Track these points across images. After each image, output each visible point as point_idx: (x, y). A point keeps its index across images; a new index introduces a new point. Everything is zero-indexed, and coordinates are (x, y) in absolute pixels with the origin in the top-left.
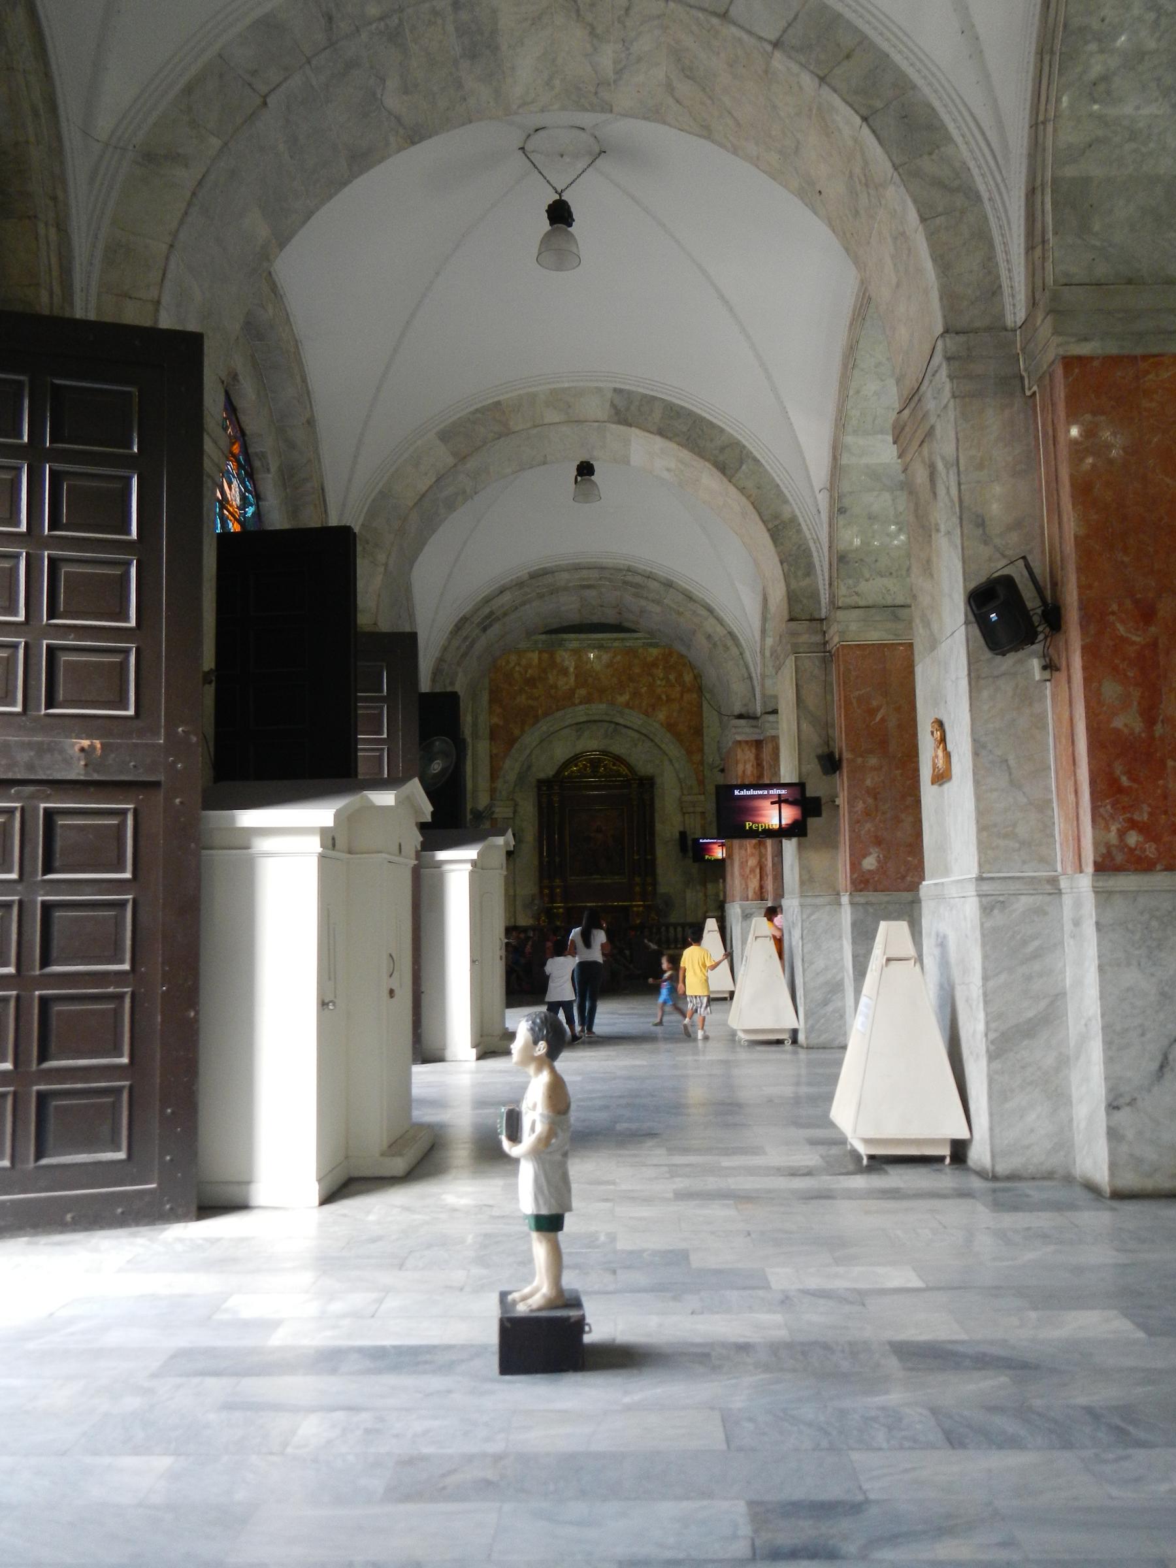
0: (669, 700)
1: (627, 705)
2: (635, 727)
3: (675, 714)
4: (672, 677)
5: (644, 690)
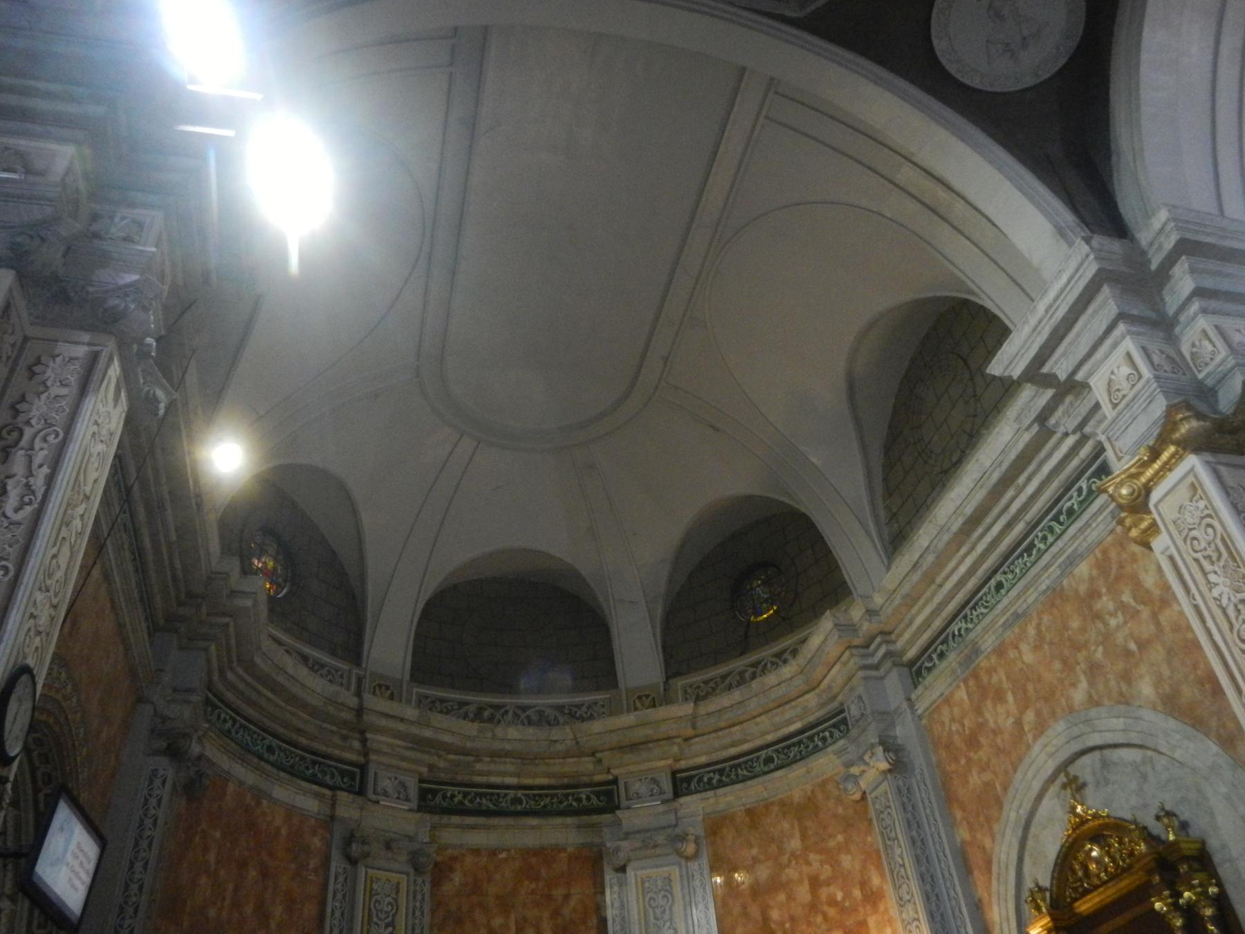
0: (1143, 645)
1: (1093, 702)
2: (1120, 739)
3: (1166, 672)
4: (1126, 598)
5: (1099, 654)
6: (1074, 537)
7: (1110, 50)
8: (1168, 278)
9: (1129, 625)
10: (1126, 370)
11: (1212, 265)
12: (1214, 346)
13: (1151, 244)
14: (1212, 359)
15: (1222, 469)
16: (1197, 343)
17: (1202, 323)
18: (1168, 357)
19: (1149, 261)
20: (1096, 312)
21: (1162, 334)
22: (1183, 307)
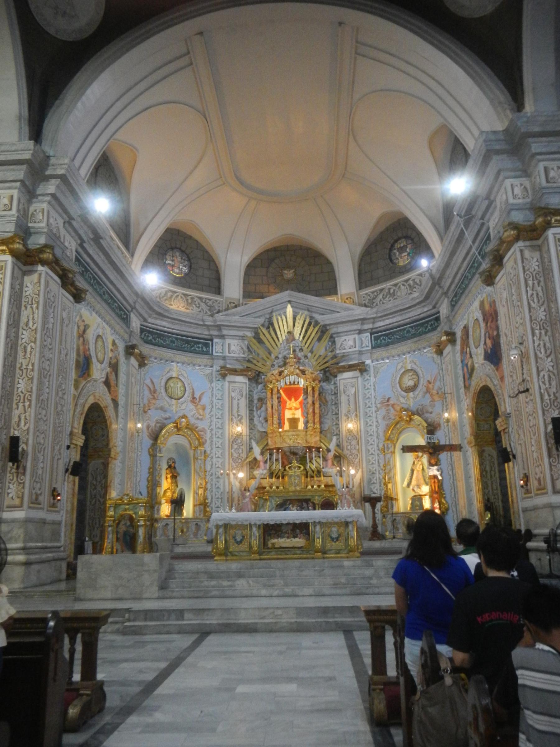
7: (89, 59)
8: (48, 181)
10: (6, 201)
11: (64, 188)
12: (43, 218)
13: (53, 165)
14: (38, 222)
15: (16, 267)
16: (38, 211)
17: (45, 205)
18: (24, 208)
19: (47, 169)
20: (14, 170)
21: (28, 197)
22: (43, 195)
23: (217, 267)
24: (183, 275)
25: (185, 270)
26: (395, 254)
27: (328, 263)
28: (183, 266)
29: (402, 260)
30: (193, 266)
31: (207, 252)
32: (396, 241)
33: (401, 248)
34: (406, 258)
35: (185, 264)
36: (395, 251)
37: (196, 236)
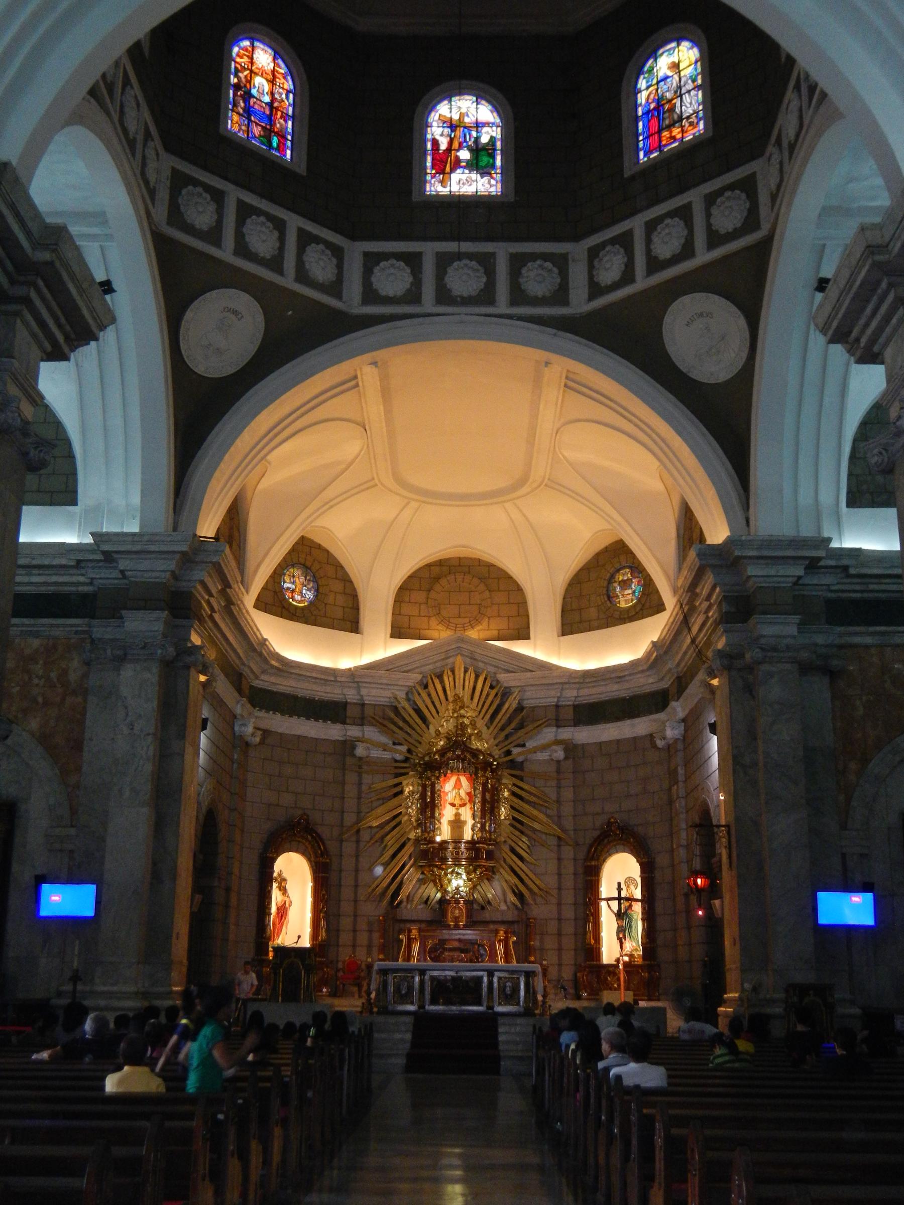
4: (53, 675)
6: (43, 625)
9: (46, 689)
23: (355, 590)
24: (306, 604)
25: (310, 595)
26: (615, 589)
27: (519, 589)
28: (307, 590)
29: (626, 599)
30: (321, 590)
31: (342, 567)
32: (618, 571)
33: (623, 581)
34: (630, 597)
35: (309, 587)
36: (616, 585)
37: (325, 544)
